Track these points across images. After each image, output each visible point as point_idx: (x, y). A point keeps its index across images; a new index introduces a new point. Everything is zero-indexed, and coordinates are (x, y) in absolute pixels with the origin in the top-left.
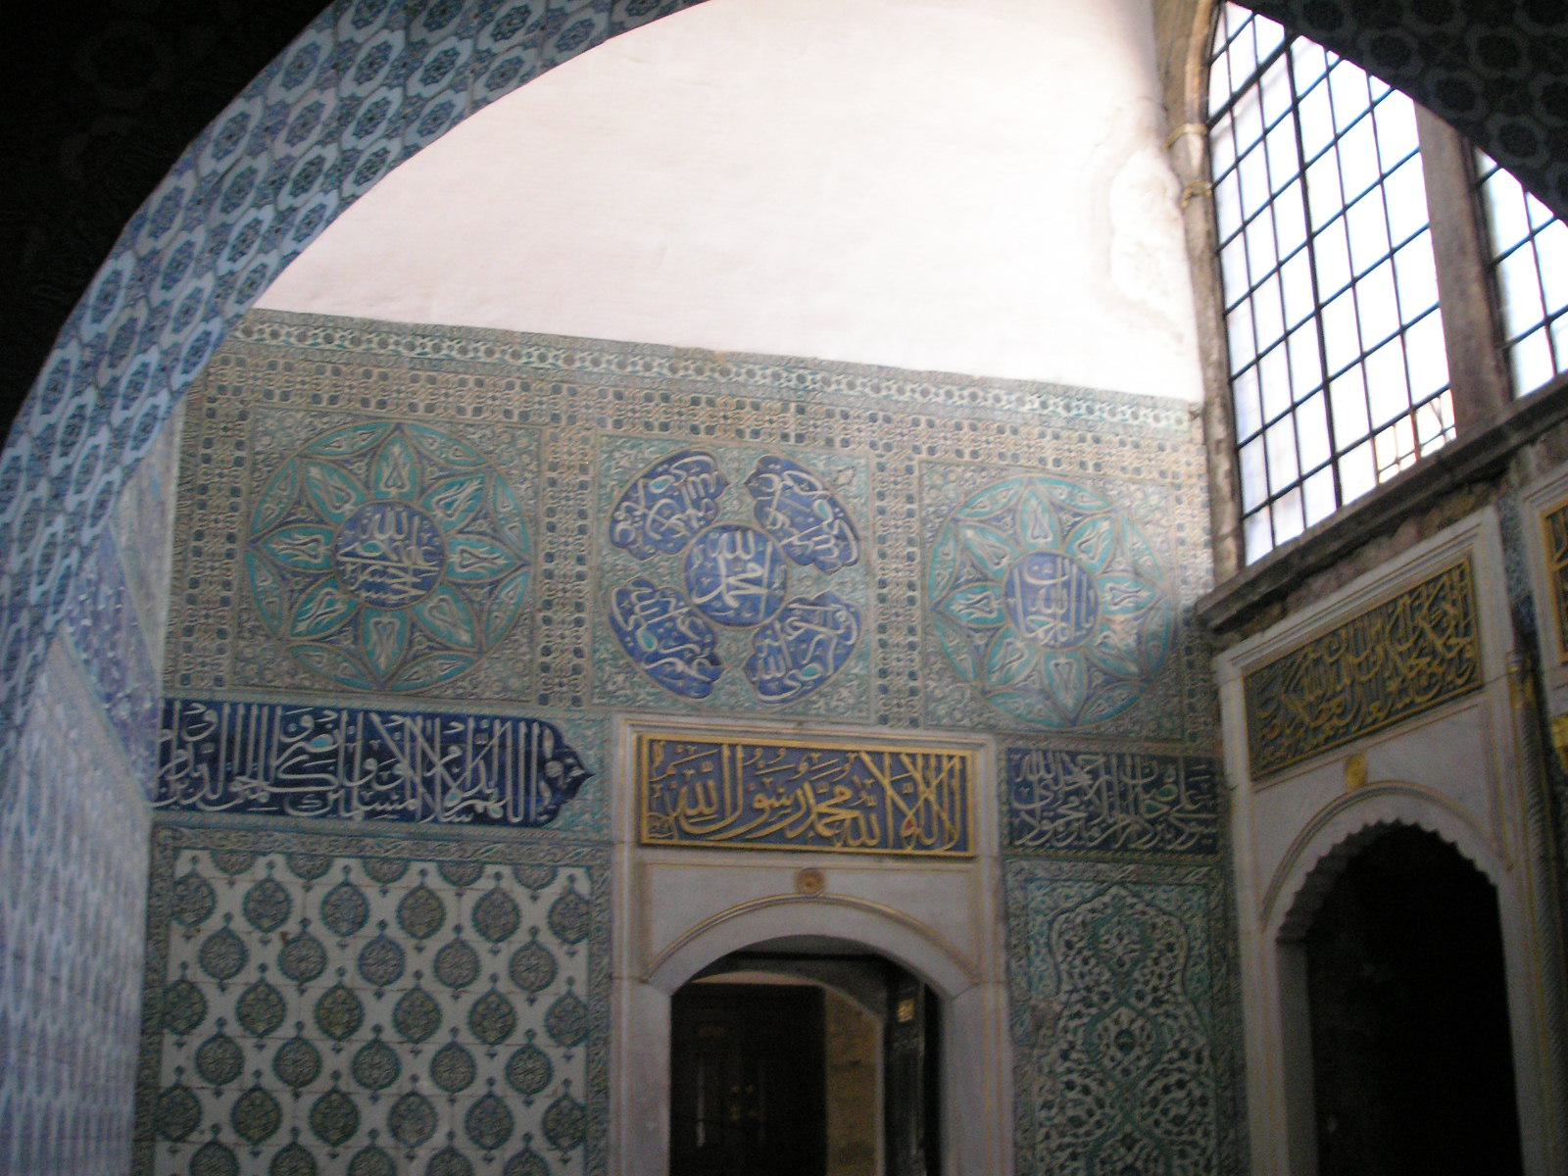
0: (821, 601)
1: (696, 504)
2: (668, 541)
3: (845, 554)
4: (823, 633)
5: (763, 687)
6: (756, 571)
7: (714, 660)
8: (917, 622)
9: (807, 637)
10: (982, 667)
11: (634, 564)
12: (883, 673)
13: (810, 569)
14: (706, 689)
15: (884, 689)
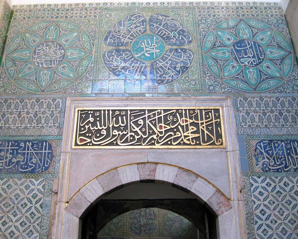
0: (152, 223)
1: (139, 214)
2: (136, 218)
3: (155, 218)
4: (152, 227)
5: (146, 233)
6: (145, 220)
7: (141, 230)
8: (163, 225)
9: (151, 227)
10: (170, 230)
11: (132, 221)
12: (159, 231)
13: (151, 220)
14: (140, 234)
15: (159, 233)
